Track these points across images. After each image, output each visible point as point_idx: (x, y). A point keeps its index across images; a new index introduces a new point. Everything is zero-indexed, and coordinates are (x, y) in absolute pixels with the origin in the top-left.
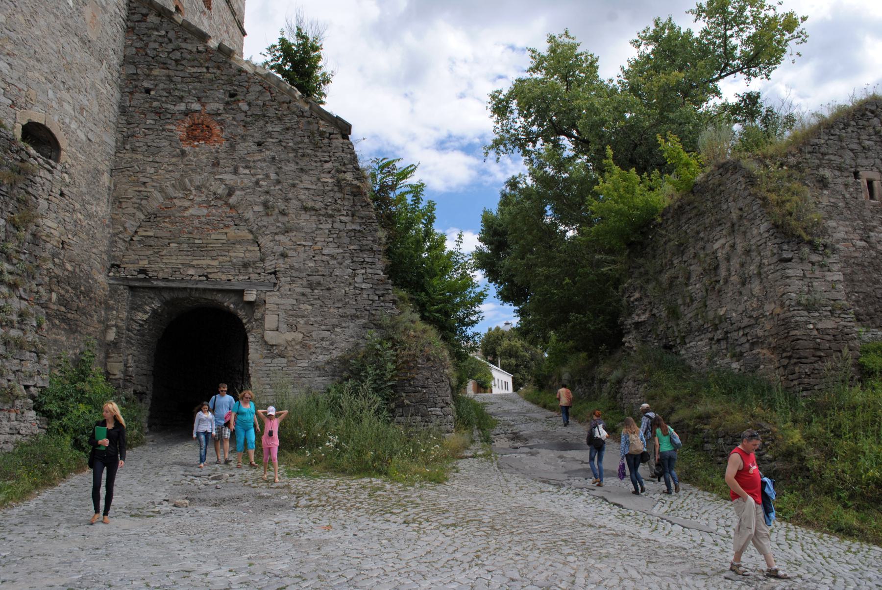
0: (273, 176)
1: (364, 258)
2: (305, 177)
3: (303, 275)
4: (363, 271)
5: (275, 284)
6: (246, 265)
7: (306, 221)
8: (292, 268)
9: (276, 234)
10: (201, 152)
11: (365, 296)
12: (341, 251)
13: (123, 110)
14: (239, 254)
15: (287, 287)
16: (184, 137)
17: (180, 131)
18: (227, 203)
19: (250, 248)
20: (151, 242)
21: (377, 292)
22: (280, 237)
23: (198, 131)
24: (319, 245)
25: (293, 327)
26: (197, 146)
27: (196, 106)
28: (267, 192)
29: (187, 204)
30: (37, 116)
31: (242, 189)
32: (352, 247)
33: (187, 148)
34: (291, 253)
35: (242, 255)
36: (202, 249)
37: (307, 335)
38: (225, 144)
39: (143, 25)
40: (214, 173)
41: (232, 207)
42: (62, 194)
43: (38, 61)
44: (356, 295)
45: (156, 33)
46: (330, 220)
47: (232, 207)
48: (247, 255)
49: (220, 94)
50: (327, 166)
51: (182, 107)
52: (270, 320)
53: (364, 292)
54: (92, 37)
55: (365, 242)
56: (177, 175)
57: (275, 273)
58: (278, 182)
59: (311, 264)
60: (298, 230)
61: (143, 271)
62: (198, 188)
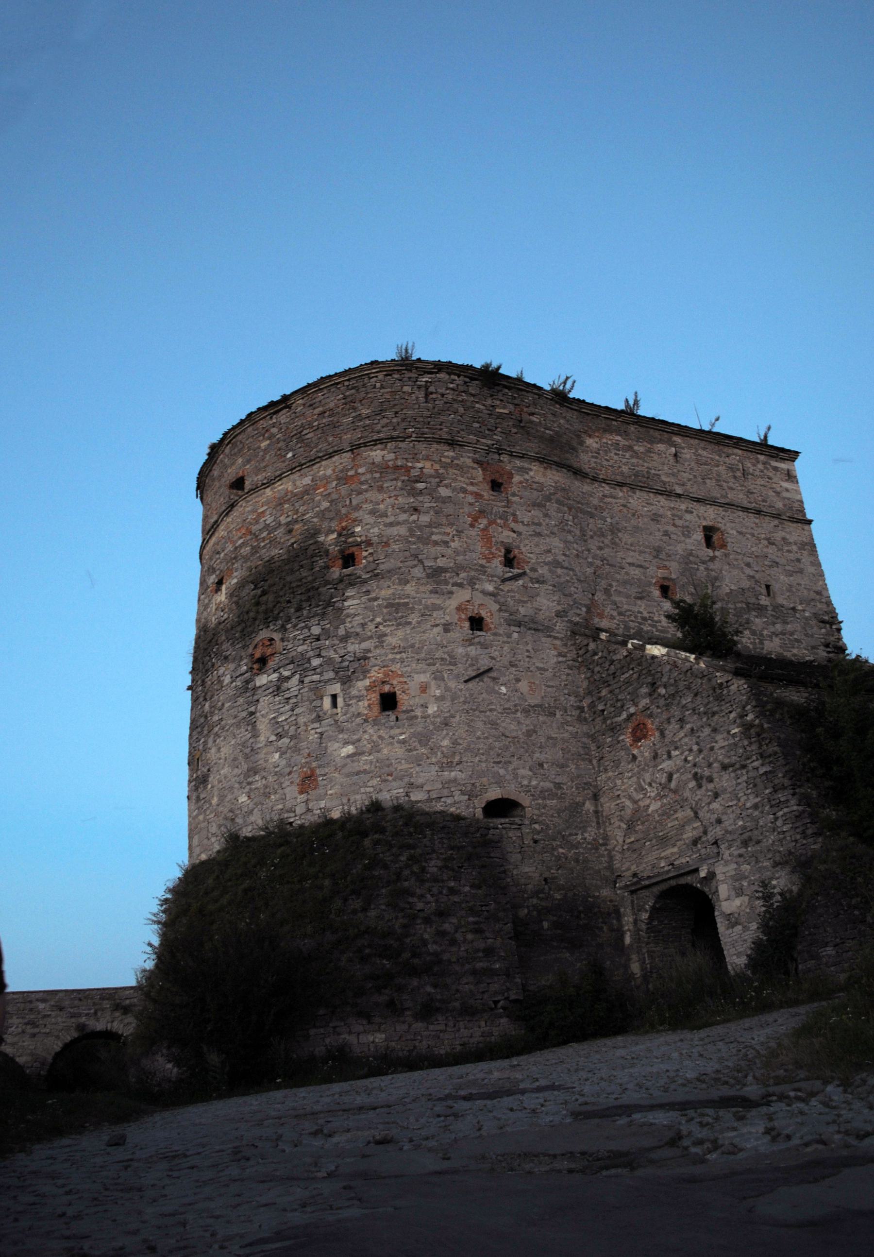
0: (695, 748)
1: (779, 798)
3: (736, 836)
4: (781, 813)
5: (718, 853)
6: (695, 842)
8: (727, 832)
9: (709, 803)
10: (644, 750)
11: (788, 838)
12: (759, 799)
14: (689, 834)
15: (727, 852)
16: (631, 742)
18: (671, 790)
19: (695, 825)
21: (798, 830)
22: (715, 806)
23: (640, 733)
24: (742, 800)
26: (641, 746)
27: (632, 710)
28: (695, 765)
29: (647, 802)
30: (494, 794)
31: (678, 771)
32: (767, 791)
33: (635, 752)
34: (724, 818)
35: (691, 835)
38: (657, 734)
39: (588, 655)
40: (656, 766)
41: (675, 792)
44: (780, 840)
45: (596, 657)
46: (744, 772)
47: (675, 792)
48: (695, 833)
50: (733, 715)
53: (787, 834)
55: (776, 781)
56: (634, 779)
57: (716, 843)
58: (700, 751)
59: (741, 823)
60: (725, 790)
62: (650, 785)
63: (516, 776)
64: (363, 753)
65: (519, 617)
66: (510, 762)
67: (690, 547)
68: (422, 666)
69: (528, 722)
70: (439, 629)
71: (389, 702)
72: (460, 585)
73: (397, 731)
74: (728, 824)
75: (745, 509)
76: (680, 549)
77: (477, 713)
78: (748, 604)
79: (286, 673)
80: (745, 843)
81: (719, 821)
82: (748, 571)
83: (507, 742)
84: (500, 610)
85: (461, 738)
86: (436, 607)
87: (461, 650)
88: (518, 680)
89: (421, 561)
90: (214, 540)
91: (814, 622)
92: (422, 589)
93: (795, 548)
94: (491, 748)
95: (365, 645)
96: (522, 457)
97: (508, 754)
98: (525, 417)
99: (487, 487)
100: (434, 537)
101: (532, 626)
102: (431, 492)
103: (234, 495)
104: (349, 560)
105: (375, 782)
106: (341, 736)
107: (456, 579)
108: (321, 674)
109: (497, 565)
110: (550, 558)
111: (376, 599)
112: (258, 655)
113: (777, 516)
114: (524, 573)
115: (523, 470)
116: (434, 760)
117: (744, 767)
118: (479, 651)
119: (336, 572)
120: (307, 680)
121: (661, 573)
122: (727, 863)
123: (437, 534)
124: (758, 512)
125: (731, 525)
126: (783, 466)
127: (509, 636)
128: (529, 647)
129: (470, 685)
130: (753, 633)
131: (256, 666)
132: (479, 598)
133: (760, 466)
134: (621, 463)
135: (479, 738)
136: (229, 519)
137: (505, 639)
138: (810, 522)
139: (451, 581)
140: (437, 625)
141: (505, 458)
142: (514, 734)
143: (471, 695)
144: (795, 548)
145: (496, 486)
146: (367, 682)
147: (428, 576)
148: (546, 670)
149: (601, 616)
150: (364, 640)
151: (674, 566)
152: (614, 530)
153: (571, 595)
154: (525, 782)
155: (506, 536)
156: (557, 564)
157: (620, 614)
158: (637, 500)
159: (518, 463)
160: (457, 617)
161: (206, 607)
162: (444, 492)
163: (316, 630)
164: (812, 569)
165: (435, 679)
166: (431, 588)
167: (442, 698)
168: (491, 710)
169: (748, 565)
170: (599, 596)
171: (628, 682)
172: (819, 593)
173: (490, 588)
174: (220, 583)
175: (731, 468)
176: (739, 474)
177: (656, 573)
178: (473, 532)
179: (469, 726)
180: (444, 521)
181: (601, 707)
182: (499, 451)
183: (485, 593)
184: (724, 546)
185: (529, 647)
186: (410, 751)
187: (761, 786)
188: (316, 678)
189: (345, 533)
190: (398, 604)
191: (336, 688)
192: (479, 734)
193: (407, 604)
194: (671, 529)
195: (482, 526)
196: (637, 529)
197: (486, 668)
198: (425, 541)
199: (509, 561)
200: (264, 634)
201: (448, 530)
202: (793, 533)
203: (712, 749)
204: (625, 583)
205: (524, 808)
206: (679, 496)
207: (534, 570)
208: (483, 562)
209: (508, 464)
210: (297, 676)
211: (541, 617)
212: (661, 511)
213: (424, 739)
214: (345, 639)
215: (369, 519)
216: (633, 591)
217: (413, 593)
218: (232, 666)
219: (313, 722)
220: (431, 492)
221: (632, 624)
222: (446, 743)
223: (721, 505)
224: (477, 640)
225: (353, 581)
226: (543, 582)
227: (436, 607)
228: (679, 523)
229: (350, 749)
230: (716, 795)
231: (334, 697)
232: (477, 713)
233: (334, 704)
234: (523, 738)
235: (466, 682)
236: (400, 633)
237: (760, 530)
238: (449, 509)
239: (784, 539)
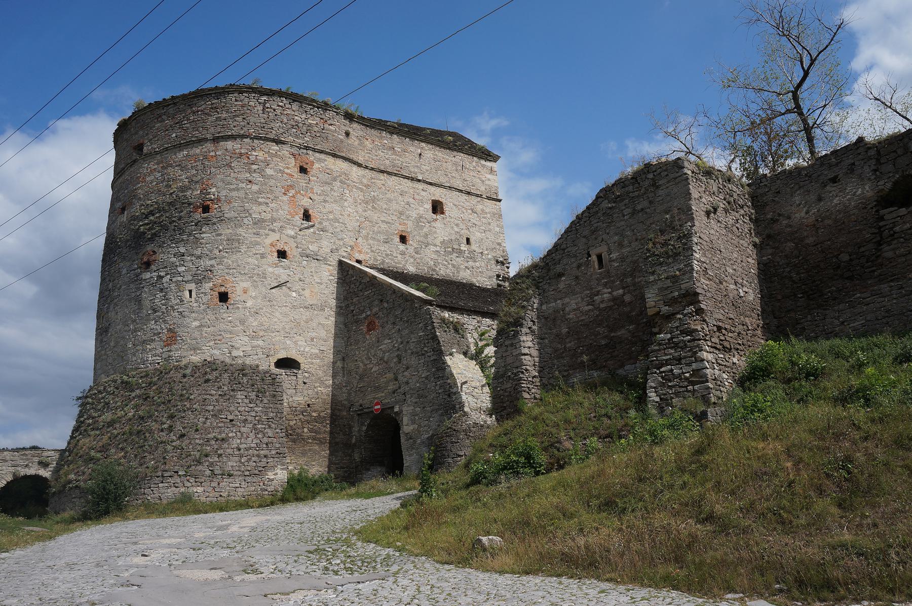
0: (399, 340)
2: (412, 336)
6: (394, 393)
7: (413, 361)
10: (371, 337)
13: (345, 325)
14: (391, 387)
17: (364, 328)
20: (363, 389)
22: (406, 373)
23: (371, 327)
25: (413, 422)
27: (369, 313)
30: (282, 355)
34: (410, 381)
36: (378, 389)
37: (420, 426)
42: (305, 383)
49: (376, 302)
51: (364, 315)
52: (405, 420)
54: (315, 302)
61: (361, 406)
64: (205, 326)
65: (308, 252)
67: (421, 212)
69: (308, 313)
70: (258, 256)
71: (224, 297)
72: (273, 231)
73: (225, 315)
74: (411, 385)
75: (461, 191)
76: (414, 214)
78: (453, 249)
79: (162, 274)
80: (420, 397)
81: (407, 383)
82: (456, 229)
84: (297, 247)
86: (258, 243)
87: (270, 270)
88: (303, 290)
90: (121, 180)
91: (493, 262)
92: (250, 231)
93: (489, 215)
94: (284, 328)
95: (213, 262)
96: (321, 152)
98: (326, 126)
99: (297, 170)
100: (260, 200)
101: (315, 257)
102: (261, 172)
103: (135, 156)
104: (206, 209)
105: (212, 343)
106: (193, 315)
108: (183, 276)
109: (298, 219)
110: (331, 217)
111: (220, 235)
112: (145, 259)
113: (481, 196)
114: (313, 226)
115: (320, 160)
117: (423, 355)
118: (282, 270)
119: (198, 215)
120: (174, 279)
121: (401, 228)
122: (409, 405)
124: (469, 193)
125: (448, 199)
126: (489, 164)
128: (313, 270)
129: (273, 290)
130: (454, 266)
131: (143, 266)
133: (474, 164)
134: (385, 159)
136: (132, 169)
138: (500, 201)
141: (310, 152)
144: (489, 215)
145: (303, 170)
146: (211, 284)
147: (255, 224)
148: (321, 284)
149: (360, 252)
150: (210, 259)
151: (410, 224)
152: (374, 200)
153: (342, 239)
155: (305, 202)
156: (336, 220)
157: (372, 251)
158: (392, 181)
159: (317, 155)
161: (114, 222)
162: (269, 171)
163: (182, 250)
164: (497, 229)
167: (255, 298)
169: (457, 225)
170: (360, 239)
171: (368, 297)
172: (499, 244)
173: (293, 233)
174: (123, 210)
175: (455, 164)
176: (460, 168)
177: (398, 228)
178: (285, 198)
181: (352, 308)
182: (307, 148)
184: (443, 213)
185: (313, 270)
187: (430, 366)
188: (180, 279)
189: (205, 192)
191: (192, 286)
194: (411, 200)
196: (390, 200)
199: (307, 216)
200: (149, 248)
201: (269, 196)
202: (490, 206)
203: (408, 342)
204: (379, 232)
205: (299, 364)
206: (419, 181)
207: (320, 223)
209: (312, 156)
210: (169, 276)
211: (321, 252)
212: (406, 189)
213: (242, 322)
214: (199, 257)
215: (220, 184)
216: (382, 237)
218: (128, 264)
219: (177, 304)
220: (261, 172)
221: (379, 258)
223: (445, 187)
225: (207, 221)
226: (326, 231)
227: (258, 243)
228: (417, 197)
229: (197, 323)
230: (408, 368)
231: (190, 291)
233: (191, 296)
237: (468, 204)
238: (272, 182)
239: (482, 210)
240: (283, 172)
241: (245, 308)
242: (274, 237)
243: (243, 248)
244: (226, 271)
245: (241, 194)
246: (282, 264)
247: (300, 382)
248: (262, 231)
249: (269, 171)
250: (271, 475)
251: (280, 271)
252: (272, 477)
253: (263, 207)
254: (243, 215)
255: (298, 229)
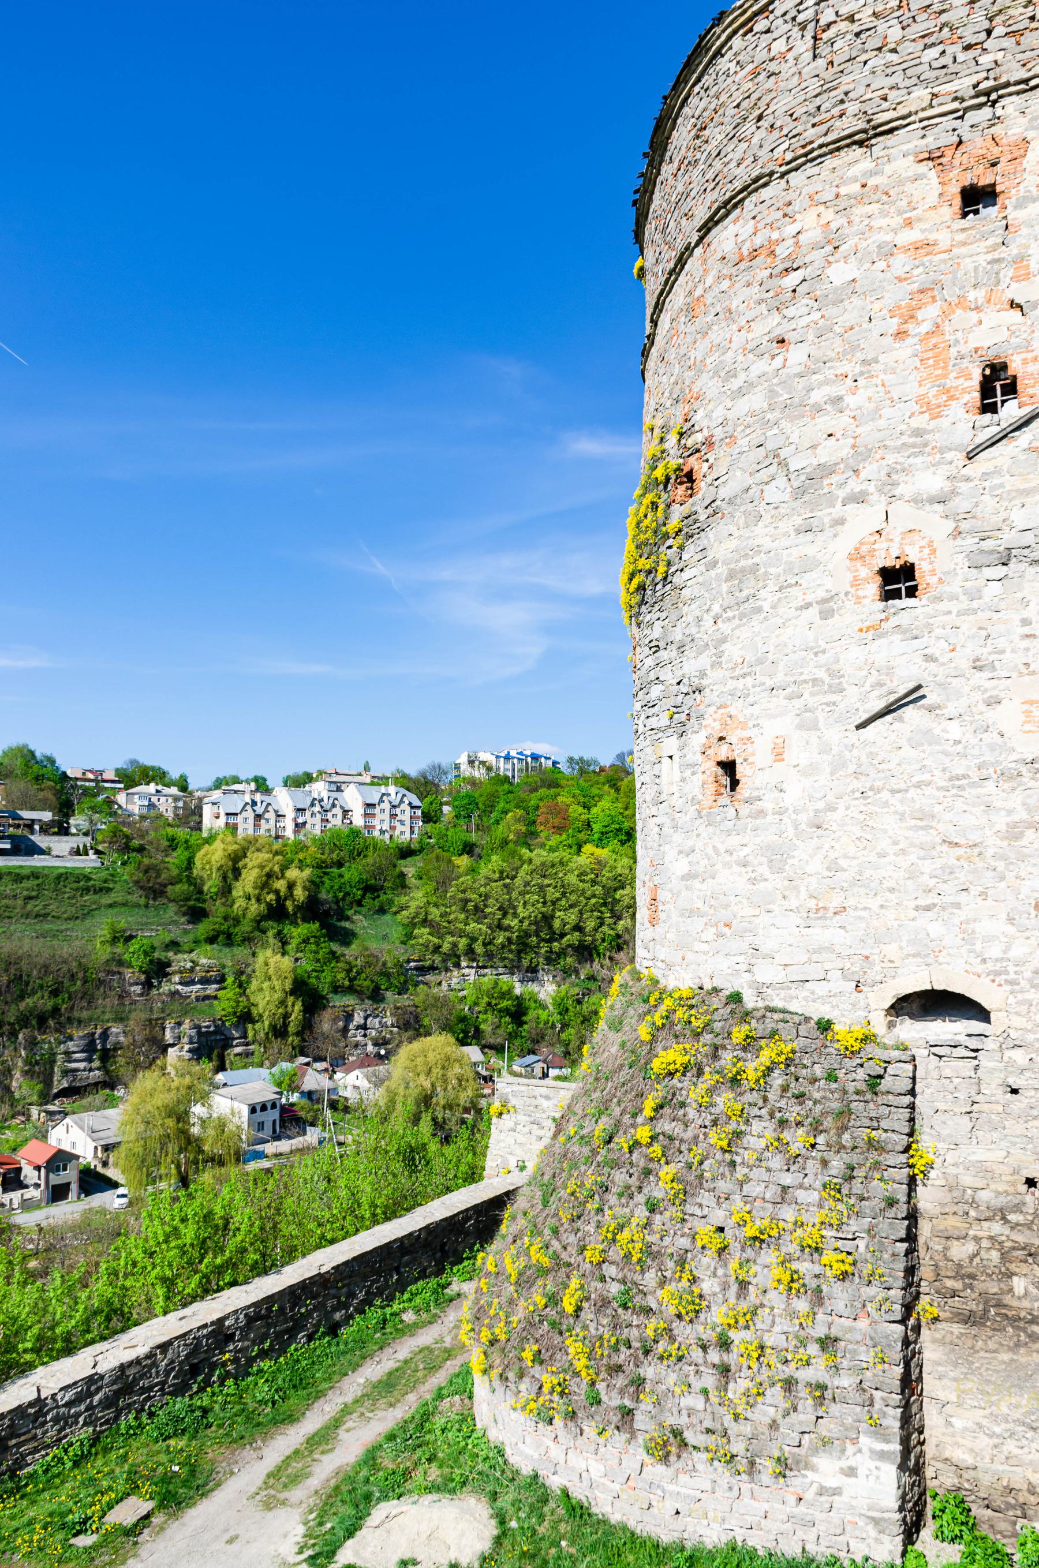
43: (892, 890)
63: (969, 937)
65: (1009, 538)
66: (957, 906)
68: (780, 699)
69: (1016, 800)
70: (814, 611)
72: (860, 499)
73: (734, 841)
77: (885, 795)
83: (950, 856)
84: (957, 533)
85: (846, 856)
86: (808, 565)
88: (994, 702)
89: (783, 464)
92: (786, 526)
94: (912, 874)
97: (949, 889)
107: (855, 486)
111: (715, 563)
116: (793, 903)
123: (821, 384)
127: (974, 595)
132: (904, 515)
135: (882, 855)
137: (964, 603)
139: (841, 494)
140: (808, 606)
142: (974, 837)
143: (872, 755)
147: (799, 492)
154: (995, 951)
160: (850, 577)
165: (800, 727)
166: (798, 521)
167: (812, 770)
168: (918, 785)
173: (933, 482)
178: (904, 350)
179: (864, 826)
180: (838, 344)
182: (989, 96)
183: (917, 501)
186: (753, 881)
190: (743, 570)
192: (884, 844)
193: (754, 569)
195: (925, 327)
197: (911, 686)
198: (798, 408)
201: (844, 367)
208: (921, 421)
217: (767, 543)
222: (816, 866)
224: (894, 621)
227: (808, 565)
232: (885, 795)
234: (993, 844)
235: (861, 726)
236: (745, 633)
238: (851, 312)
240: (889, 251)
241: (781, 812)
242: (862, 521)
243: (767, 598)
244: (731, 684)
245: (757, 400)
246: (904, 619)
247: (993, 1089)
248: (825, 515)
249: (839, 273)
250: (826, 1469)
251: (898, 647)
252: (831, 1483)
253: (826, 422)
254: (764, 475)
255: (960, 458)
